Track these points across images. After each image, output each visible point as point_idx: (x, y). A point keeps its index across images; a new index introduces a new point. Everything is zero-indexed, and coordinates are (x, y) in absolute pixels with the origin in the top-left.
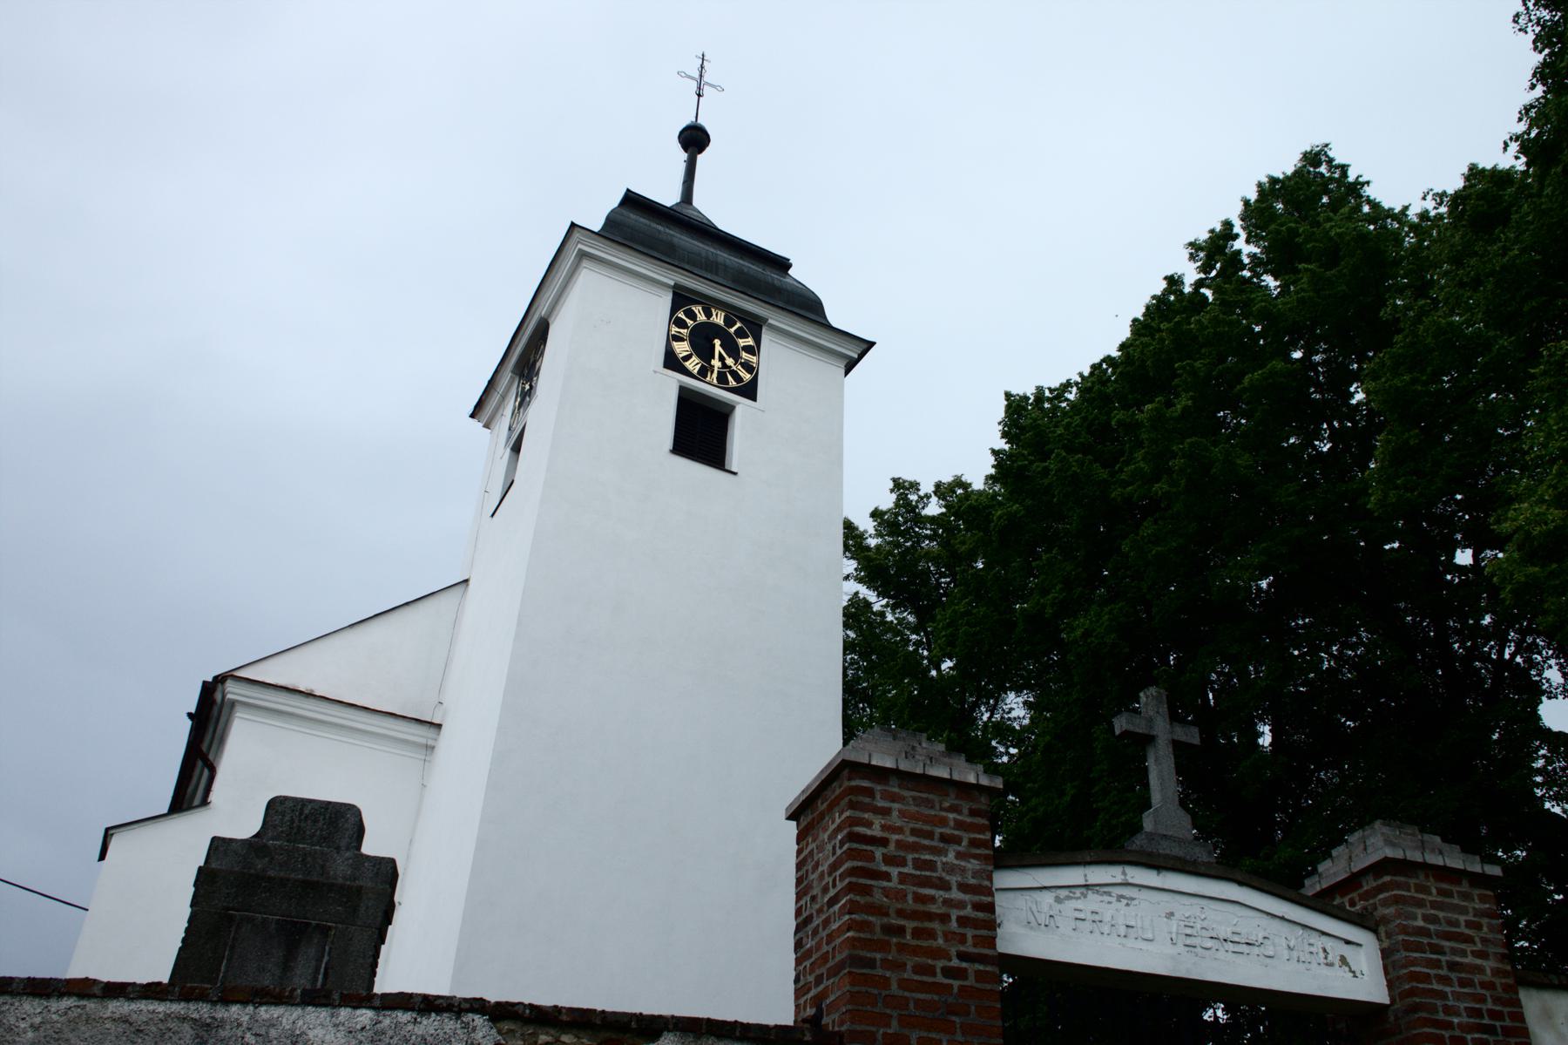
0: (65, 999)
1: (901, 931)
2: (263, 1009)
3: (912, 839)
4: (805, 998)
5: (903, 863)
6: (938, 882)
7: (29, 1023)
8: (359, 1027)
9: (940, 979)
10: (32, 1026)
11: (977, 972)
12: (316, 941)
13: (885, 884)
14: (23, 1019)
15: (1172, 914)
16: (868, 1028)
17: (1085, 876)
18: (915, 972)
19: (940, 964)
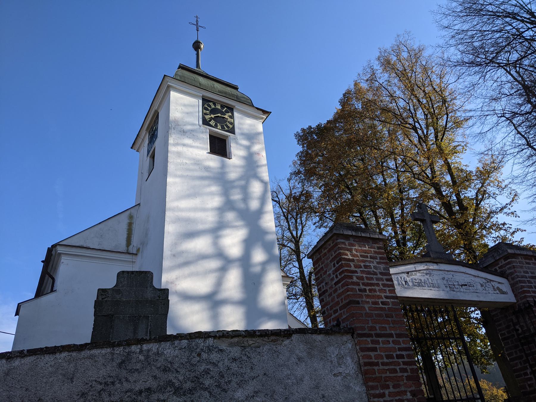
0: (63, 353)
1: (365, 290)
2: (144, 345)
3: (361, 259)
4: (330, 319)
5: (361, 267)
6: (373, 272)
7: (49, 365)
8: (183, 347)
9: (381, 305)
10: (51, 366)
11: (392, 302)
12: (144, 322)
13: (356, 274)
14: (47, 363)
15: (444, 278)
16: (362, 325)
17: (415, 267)
18: (372, 304)
19: (380, 301)
